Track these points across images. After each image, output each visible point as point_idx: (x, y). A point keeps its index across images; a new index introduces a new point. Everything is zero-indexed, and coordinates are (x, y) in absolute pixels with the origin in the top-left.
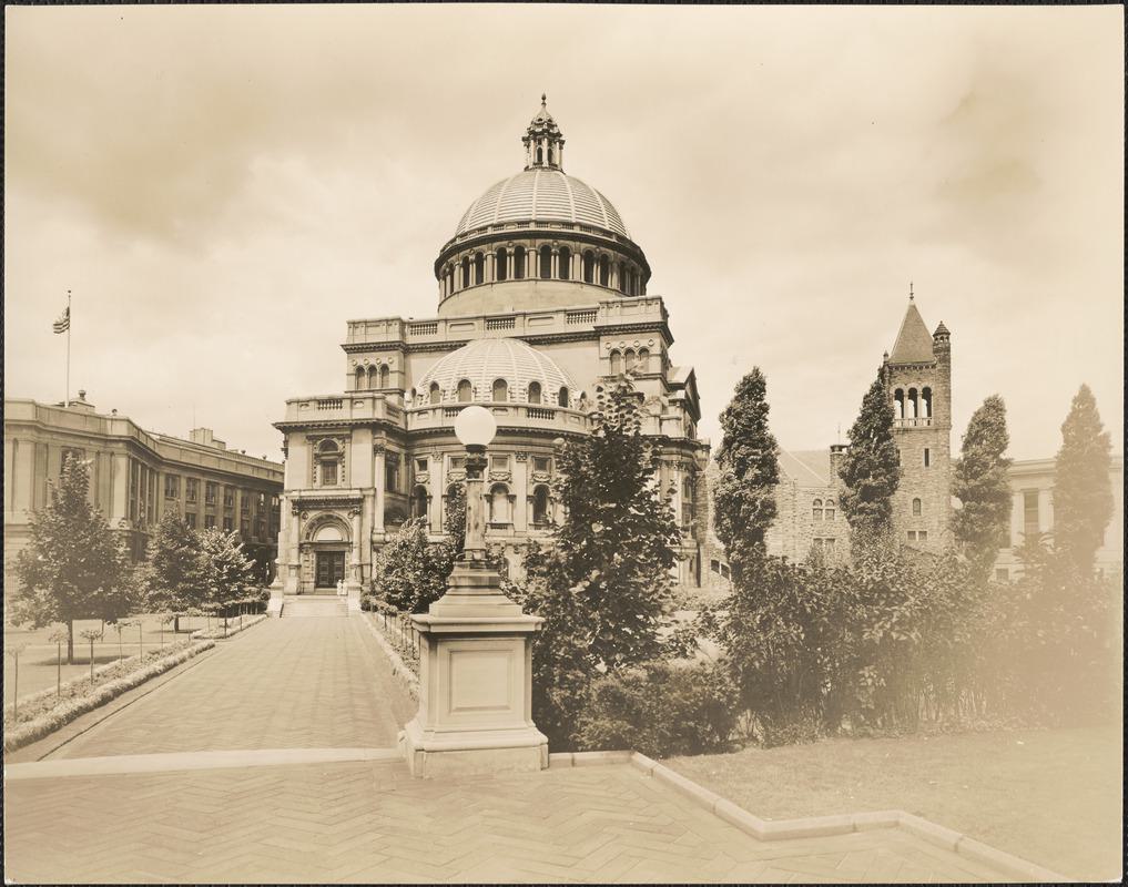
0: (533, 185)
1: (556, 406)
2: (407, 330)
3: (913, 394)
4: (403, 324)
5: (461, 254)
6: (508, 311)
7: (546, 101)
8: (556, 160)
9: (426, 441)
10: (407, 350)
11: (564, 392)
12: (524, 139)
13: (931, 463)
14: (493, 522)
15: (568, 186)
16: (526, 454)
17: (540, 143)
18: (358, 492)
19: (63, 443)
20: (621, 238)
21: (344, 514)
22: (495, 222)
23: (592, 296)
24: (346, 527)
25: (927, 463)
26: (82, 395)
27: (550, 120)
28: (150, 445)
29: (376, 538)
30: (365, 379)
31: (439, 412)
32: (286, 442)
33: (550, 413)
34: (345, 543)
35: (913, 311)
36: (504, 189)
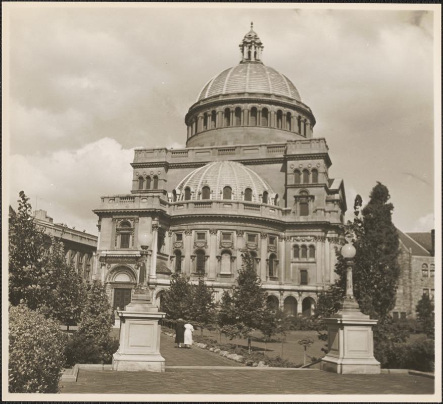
1: (261, 202)
6: (230, 145)
7: (253, 25)
11: (266, 193)
12: (240, 46)
14: (222, 273)
16: (243, 232)
17: (250, 47)
20: (297, 102)
21: (133, 266)
22: (224, 93)
23: (283, 136)
27: (255, 36)
29: (151, 281)
31: (190, 205)
34: (132, 284)
36: (229, 75)
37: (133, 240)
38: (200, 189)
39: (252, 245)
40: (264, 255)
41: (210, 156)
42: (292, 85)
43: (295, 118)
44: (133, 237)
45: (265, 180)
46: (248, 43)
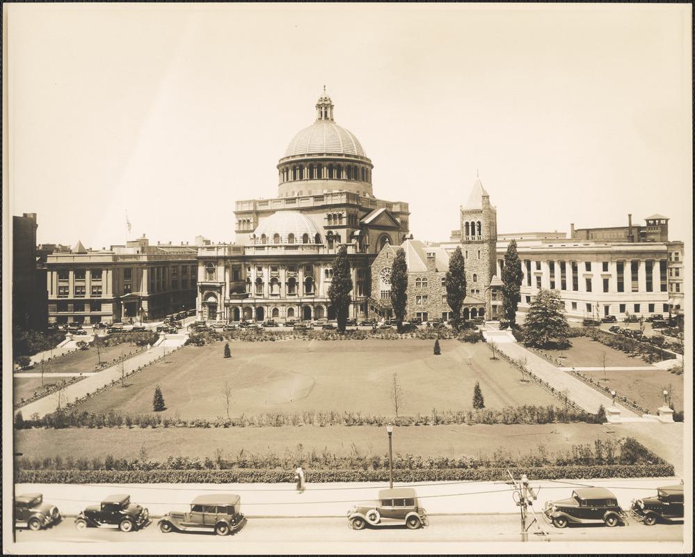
2: (257, 204)
10: (258, 213)
24: (216, 297)
30: (241, 225)
33: (296, 247)
40: (301, 277)
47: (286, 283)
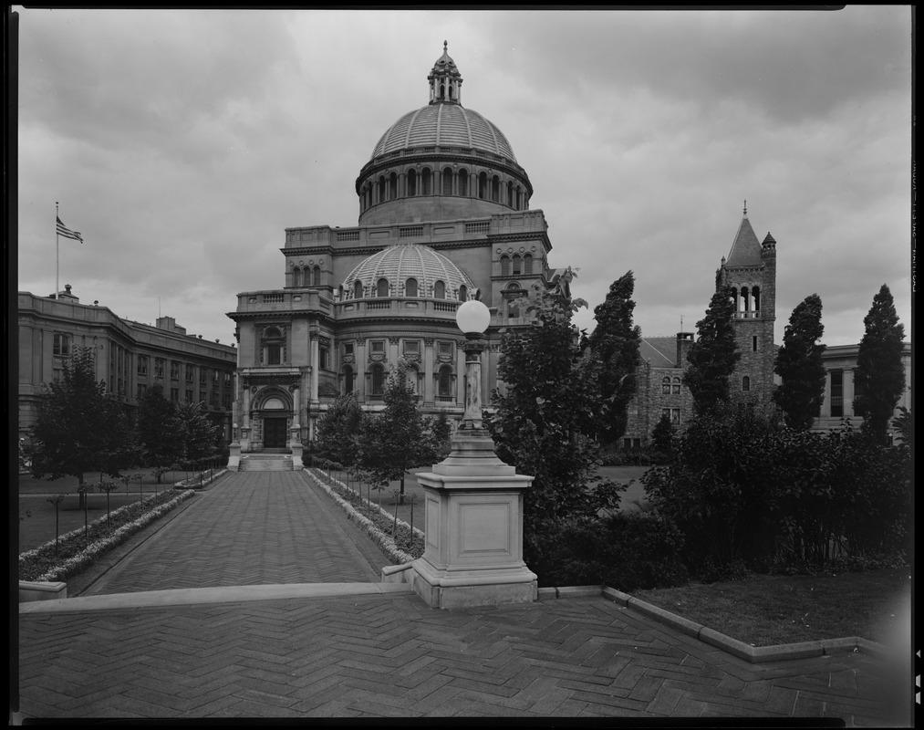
0: (437, 116)
3: (745, 292)
4: (331, 231)
5: (378, 174)
6: (417, 221)
8: (455, 96)
9: (352, 329)
10: (335, 253)
11: (463, 287)
12: (429, 78)
13: (758, 348)
15: (466, 117)
16: (433, 340)
17: (443, 81)
18: (298, 370)
19: (52, 329)
20: (509, 162)
21: (287, 388)
22: (406, 147)
23: (486, 209)
25: (755, 349)
26: (68, 288)
28: (125, 330)
31: (361, 304)
32: (237, 329)
35: (746, 223)
37: (285, 353)
38: (374, 282)
39: (445, 356)
41: (389, 237)
42: (500, 135)
43: (504, 184)
44: (285, 349)
45: (463, 271)
46: (439, 74)
47: (434, 374)
